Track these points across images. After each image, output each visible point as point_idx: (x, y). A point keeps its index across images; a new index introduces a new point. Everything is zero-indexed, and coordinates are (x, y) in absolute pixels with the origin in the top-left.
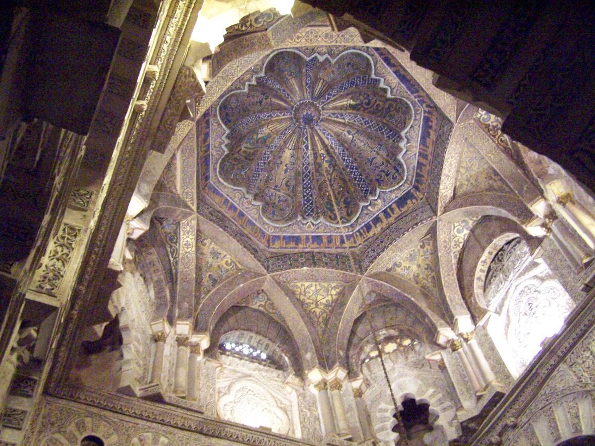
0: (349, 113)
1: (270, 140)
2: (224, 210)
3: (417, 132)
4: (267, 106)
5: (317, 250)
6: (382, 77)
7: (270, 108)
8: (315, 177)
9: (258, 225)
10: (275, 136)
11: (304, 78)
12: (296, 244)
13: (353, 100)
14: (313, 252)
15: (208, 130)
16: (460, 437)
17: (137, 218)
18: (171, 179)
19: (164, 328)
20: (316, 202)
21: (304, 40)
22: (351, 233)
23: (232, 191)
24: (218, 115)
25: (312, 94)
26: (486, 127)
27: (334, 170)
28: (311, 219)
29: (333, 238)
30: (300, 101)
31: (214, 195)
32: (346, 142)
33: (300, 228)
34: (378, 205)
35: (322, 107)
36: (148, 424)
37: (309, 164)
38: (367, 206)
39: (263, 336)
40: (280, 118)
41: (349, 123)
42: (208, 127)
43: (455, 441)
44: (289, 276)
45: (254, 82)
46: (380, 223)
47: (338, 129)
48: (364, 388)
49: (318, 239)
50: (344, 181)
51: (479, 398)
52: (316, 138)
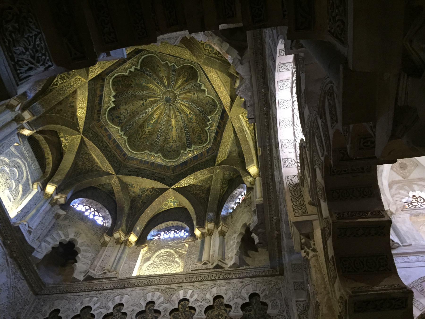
1: (160, 119)
2: (141, 166)
3: (203, 77)
4: (148, 104)
6: (166, 61)
7: (150, 104)
8: (189, 126)
10: (161, 116)
11: (153, 81)
15: (108, 133)
17: (59, 194)
18: (94, 165)
19: (105, 239)
20: (191, 139)
21: (99, 69)
24: (110, 123)
25: (164, 86)
26: (215, 55)
28: (188, 149)
29: (203, 153)
31: (133, 161)
32: (195, 100)
35: (174, 90)
36: (89, 293)
38: (209, 128)
39: (178, 221)
42: (108, 131)
43: (259, 243)
44: (183, 184)
45: (113, 100)
47: (188, 95)
48: (225, 229)
49: (195, 157)
50: (201, 120)
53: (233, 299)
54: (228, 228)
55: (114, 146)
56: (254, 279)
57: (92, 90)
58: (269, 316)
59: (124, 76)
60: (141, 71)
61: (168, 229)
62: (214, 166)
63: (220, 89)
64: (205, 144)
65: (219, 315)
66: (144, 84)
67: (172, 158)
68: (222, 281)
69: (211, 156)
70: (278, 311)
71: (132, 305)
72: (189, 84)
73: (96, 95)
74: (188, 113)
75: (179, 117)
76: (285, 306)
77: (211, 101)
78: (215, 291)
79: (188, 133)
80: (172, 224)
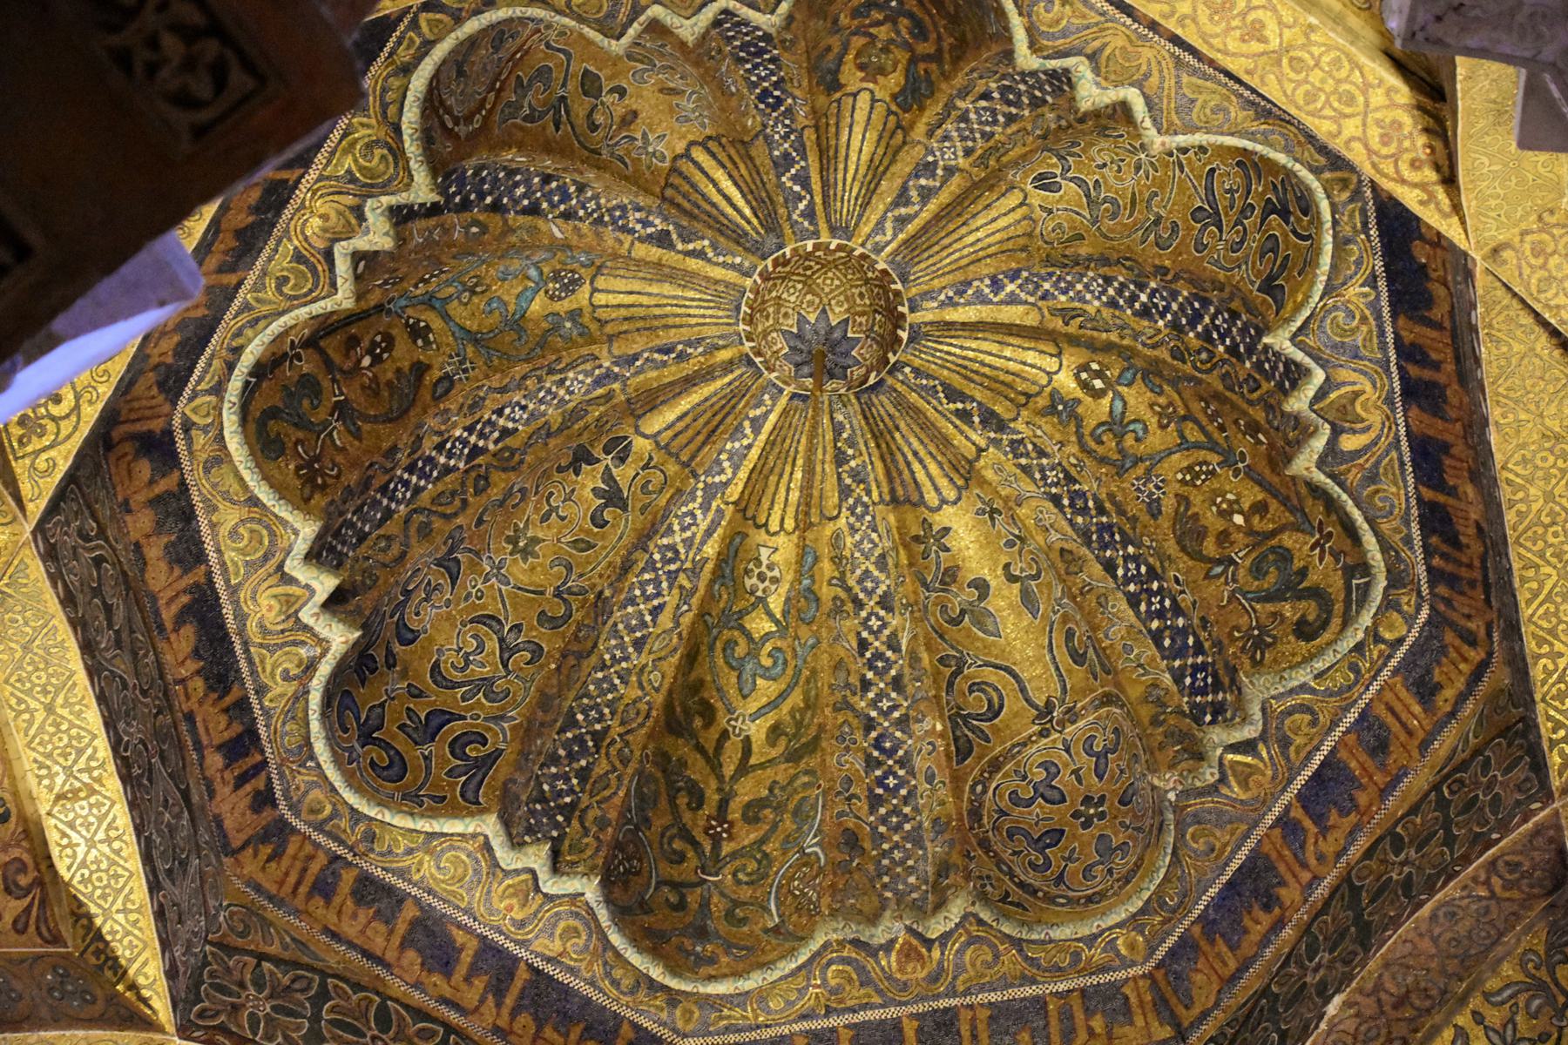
0: (930, 134)
1: (827, 567)
5: (1363, 842)
7: (672, 468)
9: (1062, 987)
10: (829, 529)
11: (609, 234)
12: (1267, 908)
13: (882, 71)
14: (1346, 879)
15: (409, 912)
22: (1424, 614)
23: (800, 981)
24: (388, 817)
27: (1174, 383)
29: (1381, 710)
30: (738, 308)
33: (1221, 820)
34: (1357, 394)
35: (833, 230)
37: (1070, 479)
40: (754, 453)
41: (982, 161)
42: (399, 899)
45: (324, 584)
46: (1448, 461)
50: (1217, 396)
52: (983, 350)
55: (514, 1013)
57: (97, 592)
59: (326, 326)
60: (465, 205)
62: (1547, 796)
63: (1255, 32)
64: (1366, 619)
66: (537, 306)
67: (1102, 895)
69: (1469, 706)
72: (949, 106)
73: (157, 613)
74: (1066, 382)
75: (994, 464)
77: (1228, 178)
79: (1153, 574)
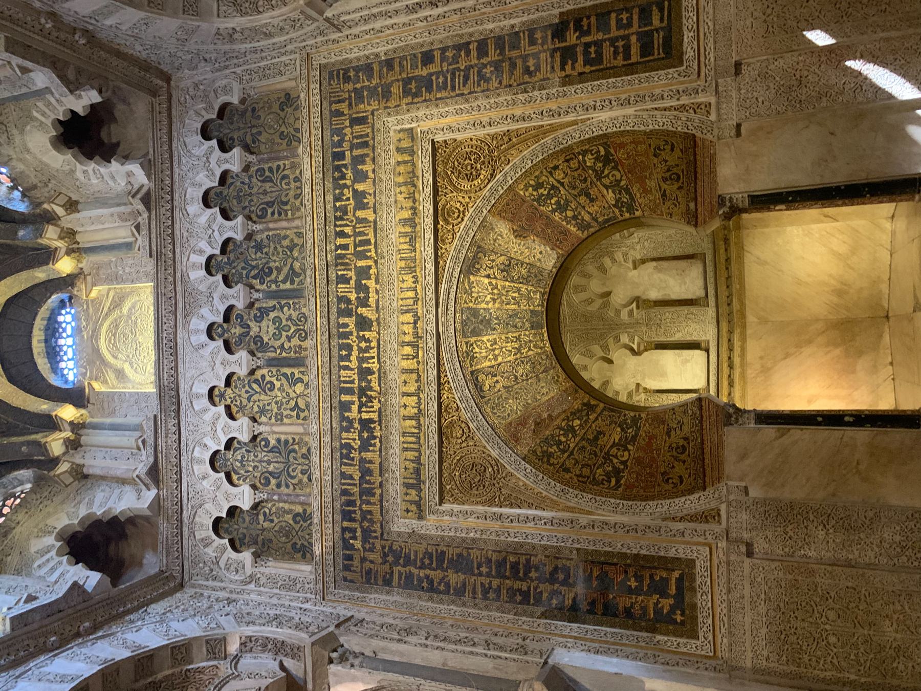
16: (93, 88)
36: (184, 470)
39: (32, 328)
43: (100, 92)
48: (62, 200)
51: (24, 70)
53: (211, 170)
54: (61, 193)
56: (175, 134)
58: (243, 101)
61: (53, 354)
65: (239, 199)
68: (176, 196)
70: (235, 83)
71: (213, 369)
76: (227, 71)
78: (195, 207)
80: (39, 341)
